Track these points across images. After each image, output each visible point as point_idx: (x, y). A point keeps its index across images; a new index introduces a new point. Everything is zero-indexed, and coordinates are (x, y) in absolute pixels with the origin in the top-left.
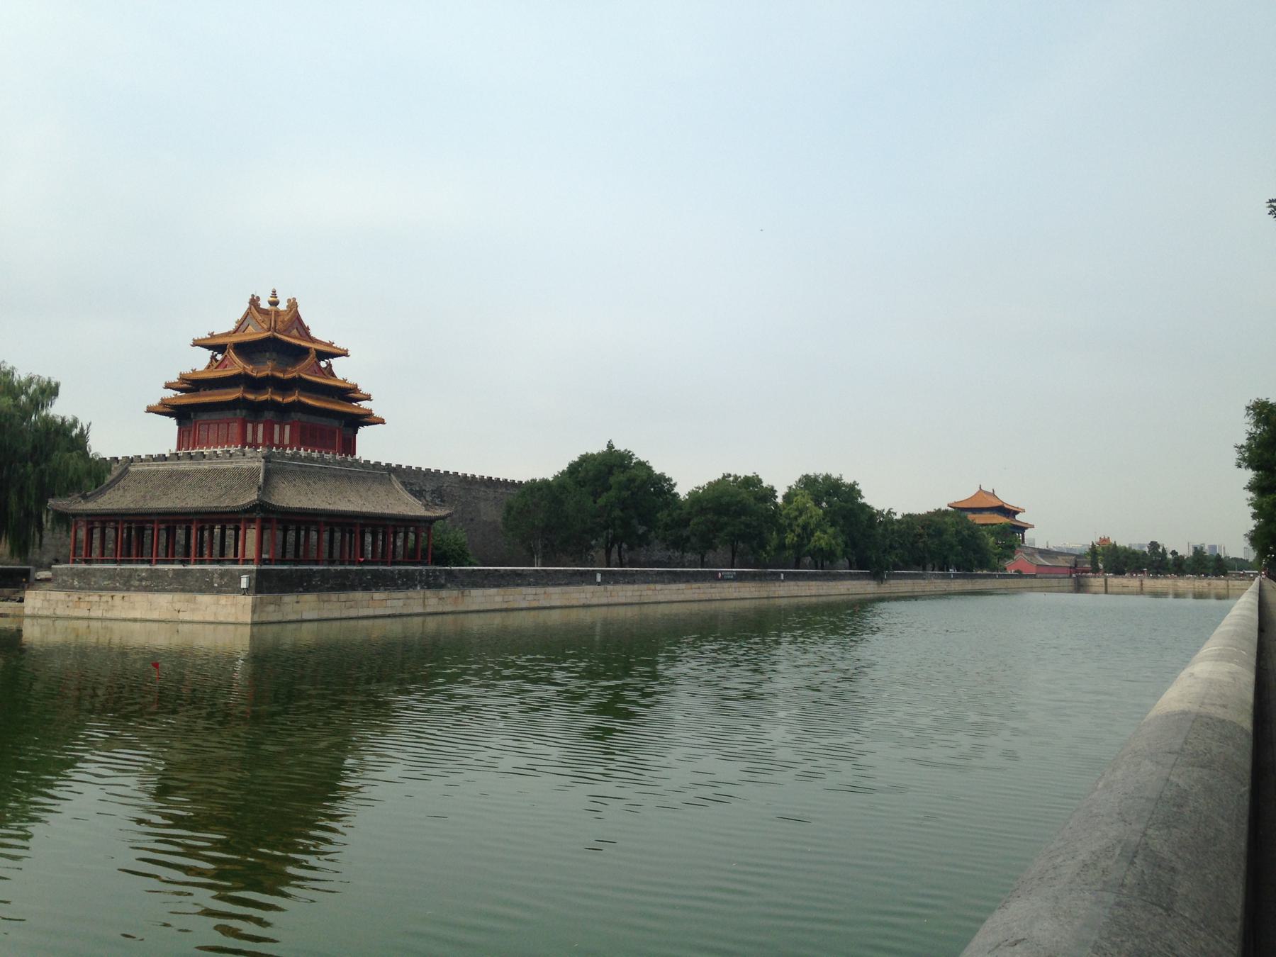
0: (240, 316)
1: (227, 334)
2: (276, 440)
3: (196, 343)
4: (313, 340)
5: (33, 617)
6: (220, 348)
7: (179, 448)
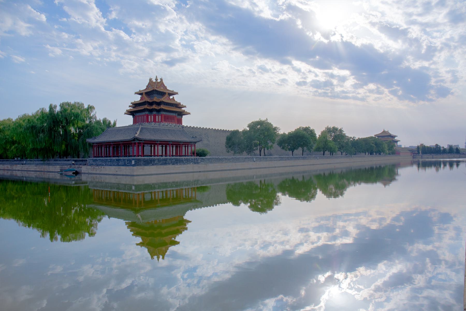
2: (157, 121)
3: (136, 93)
4: (168, 90)
5: (85, 173)
6: (141, 94)
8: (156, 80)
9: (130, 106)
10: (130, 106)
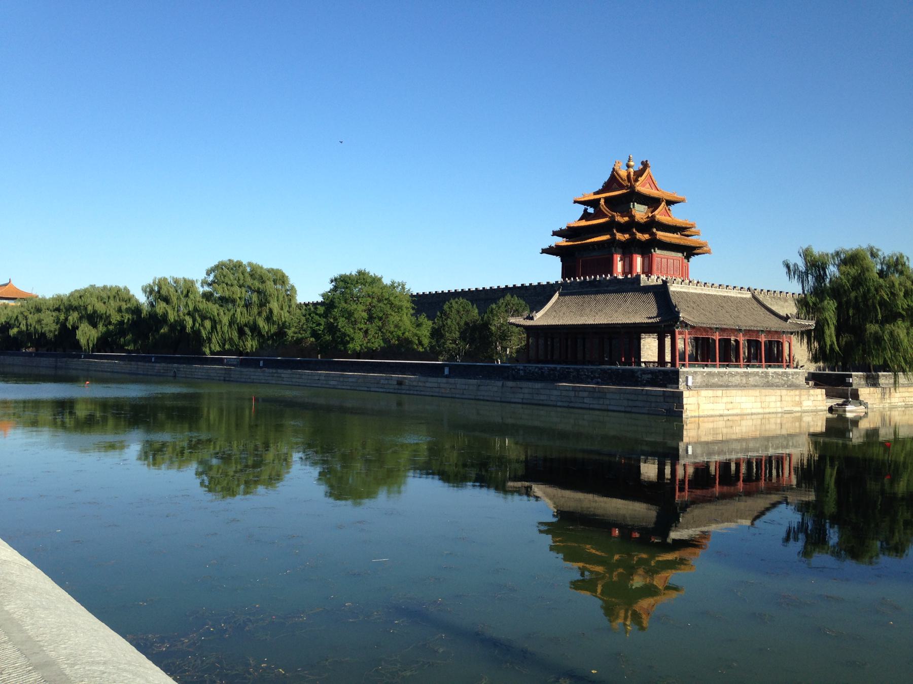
0: (606, 177)
1: (595, 193)
7: (563, 277)
8: (628, 166)
9: (555, 234)
10: (555, 234)
